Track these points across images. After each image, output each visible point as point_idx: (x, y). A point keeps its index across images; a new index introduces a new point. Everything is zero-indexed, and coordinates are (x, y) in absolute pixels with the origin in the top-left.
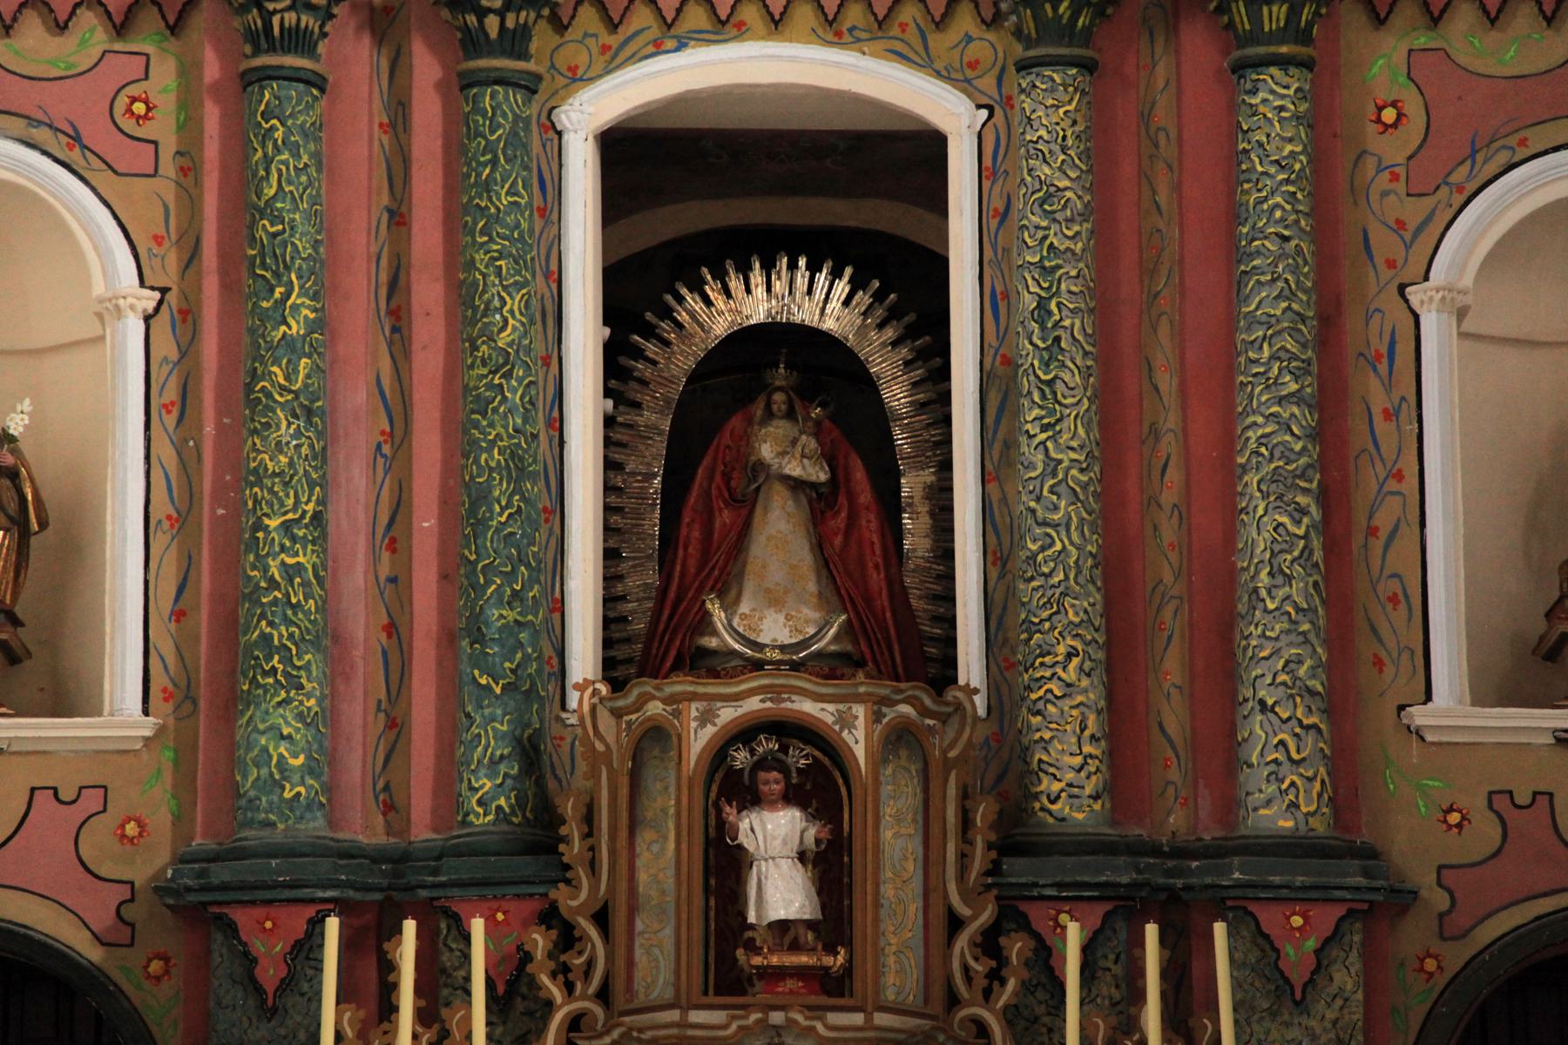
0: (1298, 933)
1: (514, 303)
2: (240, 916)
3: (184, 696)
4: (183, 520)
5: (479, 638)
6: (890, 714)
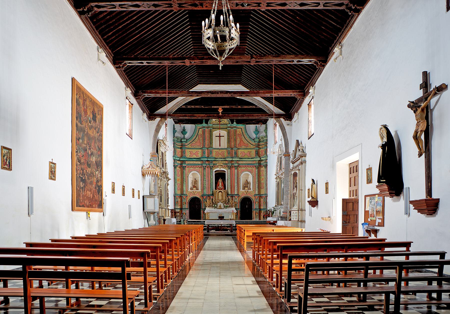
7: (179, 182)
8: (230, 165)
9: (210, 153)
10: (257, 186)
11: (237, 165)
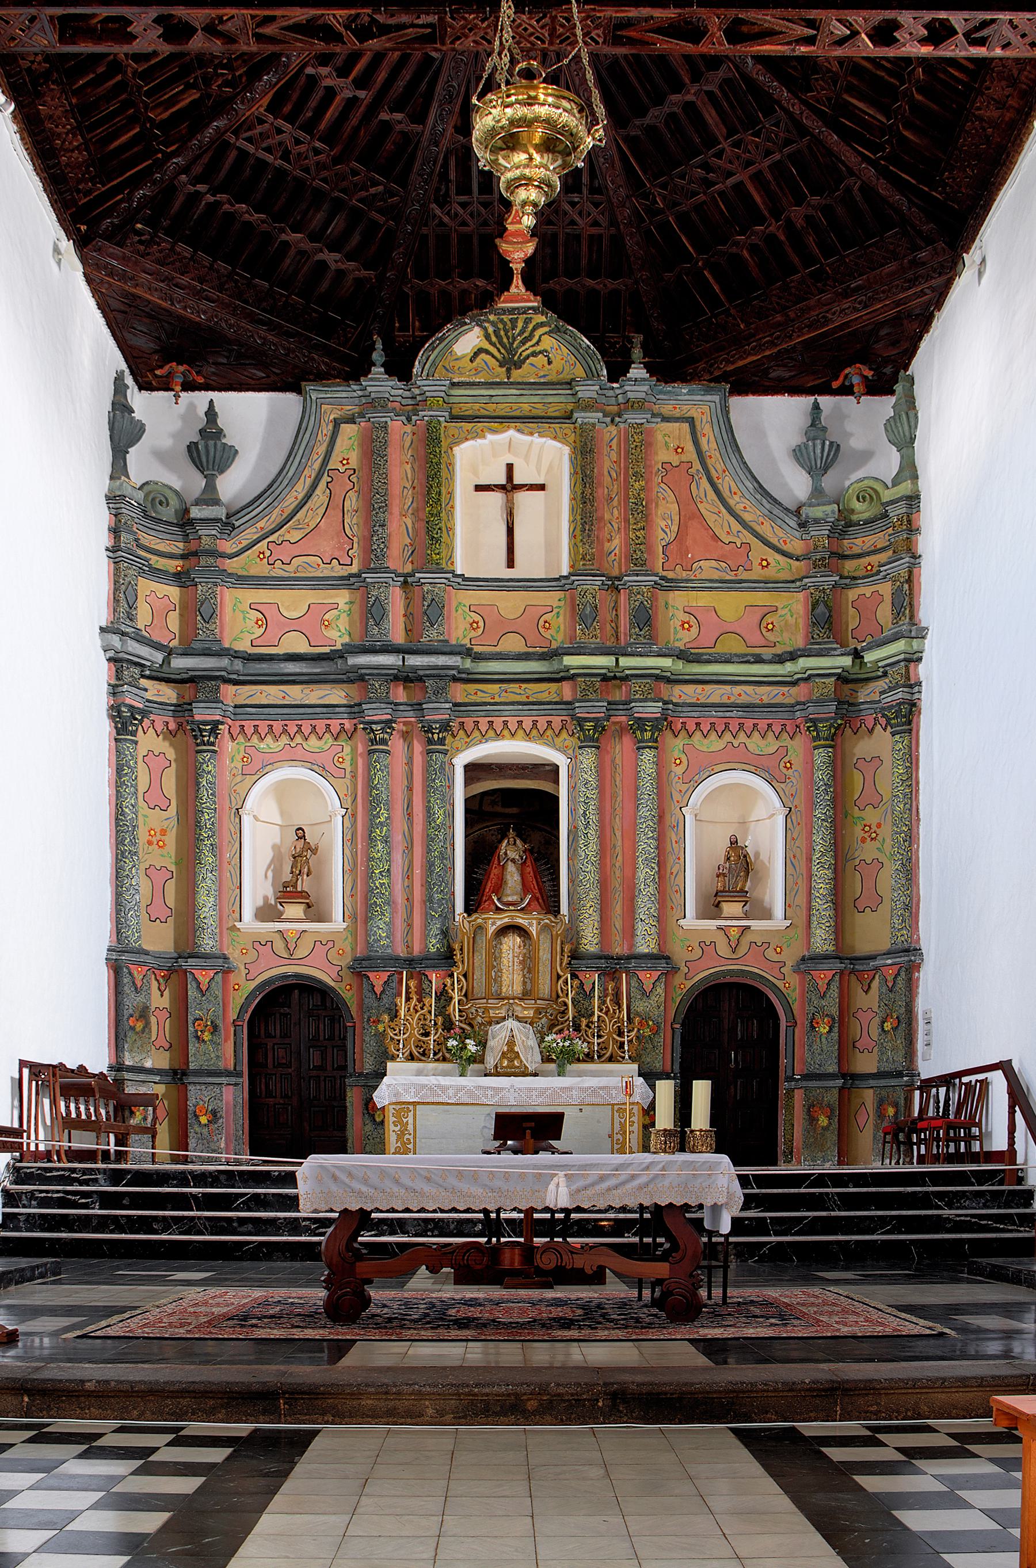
0: (648, 978)
1: (441, 812)
2: (370, 974)
3: (354, 917)
4: (353, 870)
5: (431, 902)
6: (542, 923)
7: (166, 857)
8: (597, 709)
9: (428, 611)
10: (822, 888)
11: (652, 710)
